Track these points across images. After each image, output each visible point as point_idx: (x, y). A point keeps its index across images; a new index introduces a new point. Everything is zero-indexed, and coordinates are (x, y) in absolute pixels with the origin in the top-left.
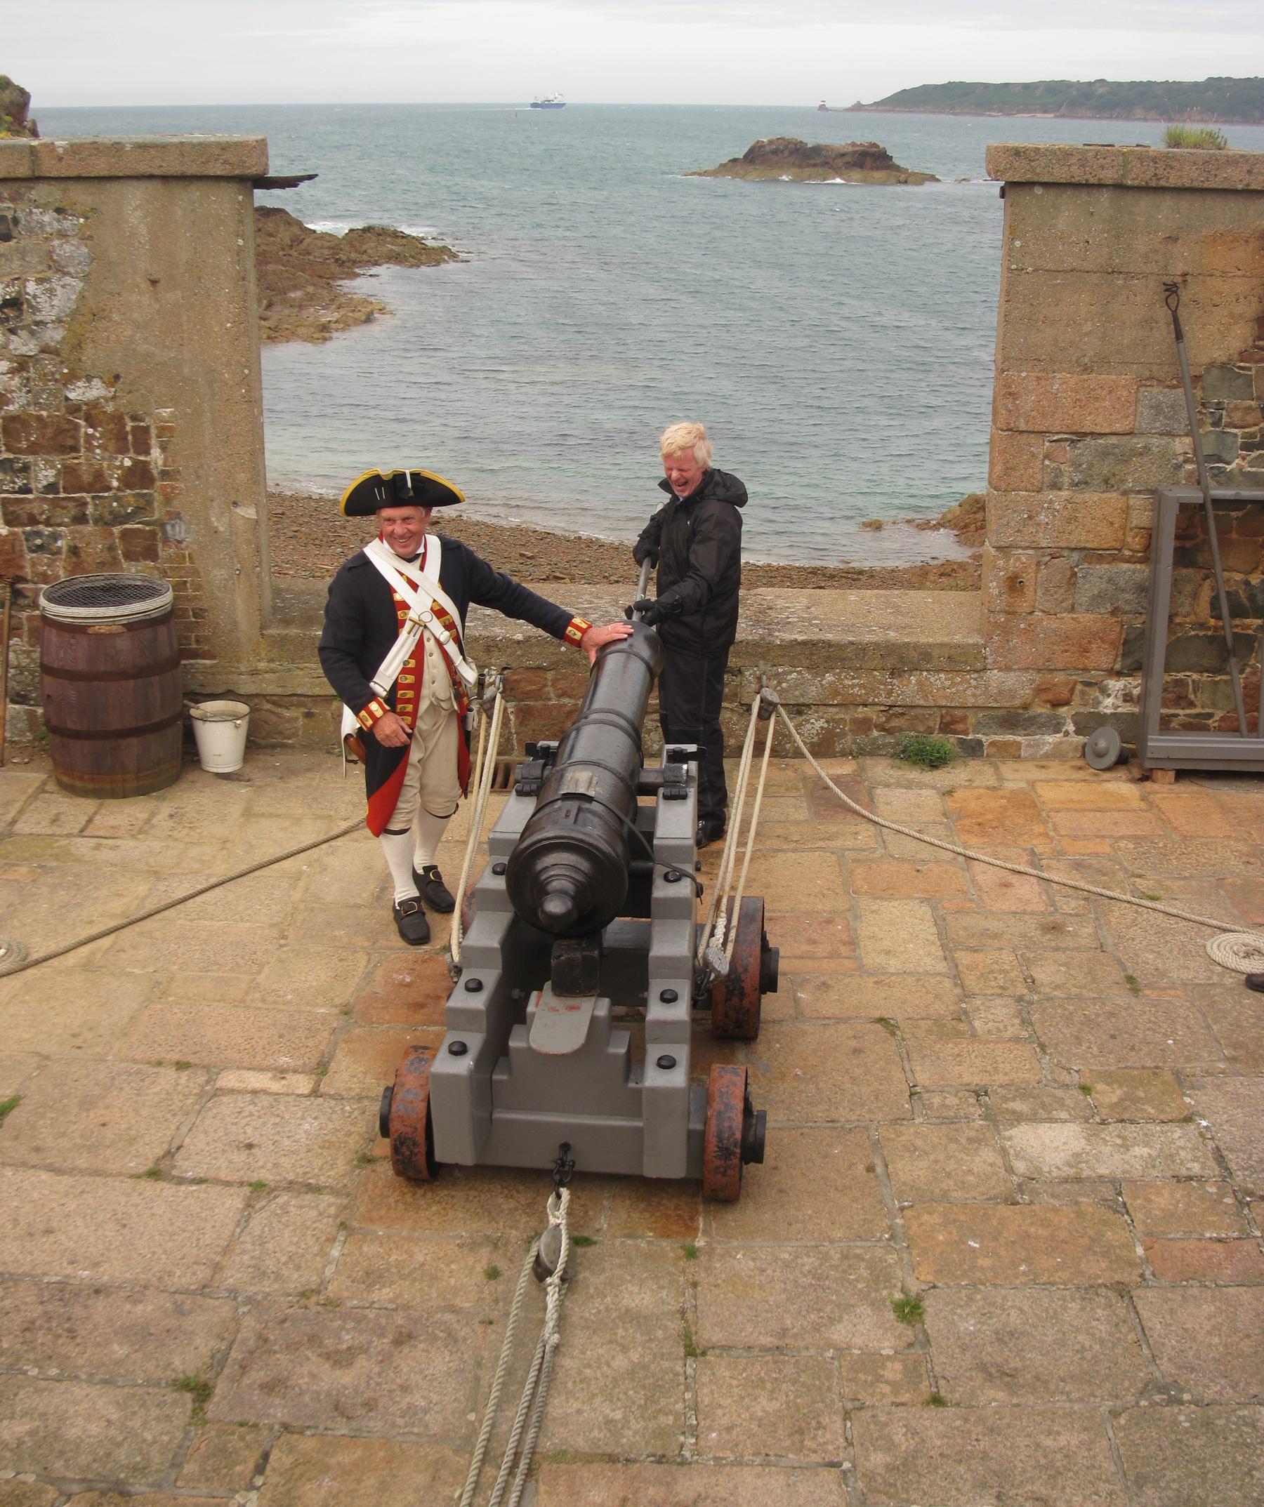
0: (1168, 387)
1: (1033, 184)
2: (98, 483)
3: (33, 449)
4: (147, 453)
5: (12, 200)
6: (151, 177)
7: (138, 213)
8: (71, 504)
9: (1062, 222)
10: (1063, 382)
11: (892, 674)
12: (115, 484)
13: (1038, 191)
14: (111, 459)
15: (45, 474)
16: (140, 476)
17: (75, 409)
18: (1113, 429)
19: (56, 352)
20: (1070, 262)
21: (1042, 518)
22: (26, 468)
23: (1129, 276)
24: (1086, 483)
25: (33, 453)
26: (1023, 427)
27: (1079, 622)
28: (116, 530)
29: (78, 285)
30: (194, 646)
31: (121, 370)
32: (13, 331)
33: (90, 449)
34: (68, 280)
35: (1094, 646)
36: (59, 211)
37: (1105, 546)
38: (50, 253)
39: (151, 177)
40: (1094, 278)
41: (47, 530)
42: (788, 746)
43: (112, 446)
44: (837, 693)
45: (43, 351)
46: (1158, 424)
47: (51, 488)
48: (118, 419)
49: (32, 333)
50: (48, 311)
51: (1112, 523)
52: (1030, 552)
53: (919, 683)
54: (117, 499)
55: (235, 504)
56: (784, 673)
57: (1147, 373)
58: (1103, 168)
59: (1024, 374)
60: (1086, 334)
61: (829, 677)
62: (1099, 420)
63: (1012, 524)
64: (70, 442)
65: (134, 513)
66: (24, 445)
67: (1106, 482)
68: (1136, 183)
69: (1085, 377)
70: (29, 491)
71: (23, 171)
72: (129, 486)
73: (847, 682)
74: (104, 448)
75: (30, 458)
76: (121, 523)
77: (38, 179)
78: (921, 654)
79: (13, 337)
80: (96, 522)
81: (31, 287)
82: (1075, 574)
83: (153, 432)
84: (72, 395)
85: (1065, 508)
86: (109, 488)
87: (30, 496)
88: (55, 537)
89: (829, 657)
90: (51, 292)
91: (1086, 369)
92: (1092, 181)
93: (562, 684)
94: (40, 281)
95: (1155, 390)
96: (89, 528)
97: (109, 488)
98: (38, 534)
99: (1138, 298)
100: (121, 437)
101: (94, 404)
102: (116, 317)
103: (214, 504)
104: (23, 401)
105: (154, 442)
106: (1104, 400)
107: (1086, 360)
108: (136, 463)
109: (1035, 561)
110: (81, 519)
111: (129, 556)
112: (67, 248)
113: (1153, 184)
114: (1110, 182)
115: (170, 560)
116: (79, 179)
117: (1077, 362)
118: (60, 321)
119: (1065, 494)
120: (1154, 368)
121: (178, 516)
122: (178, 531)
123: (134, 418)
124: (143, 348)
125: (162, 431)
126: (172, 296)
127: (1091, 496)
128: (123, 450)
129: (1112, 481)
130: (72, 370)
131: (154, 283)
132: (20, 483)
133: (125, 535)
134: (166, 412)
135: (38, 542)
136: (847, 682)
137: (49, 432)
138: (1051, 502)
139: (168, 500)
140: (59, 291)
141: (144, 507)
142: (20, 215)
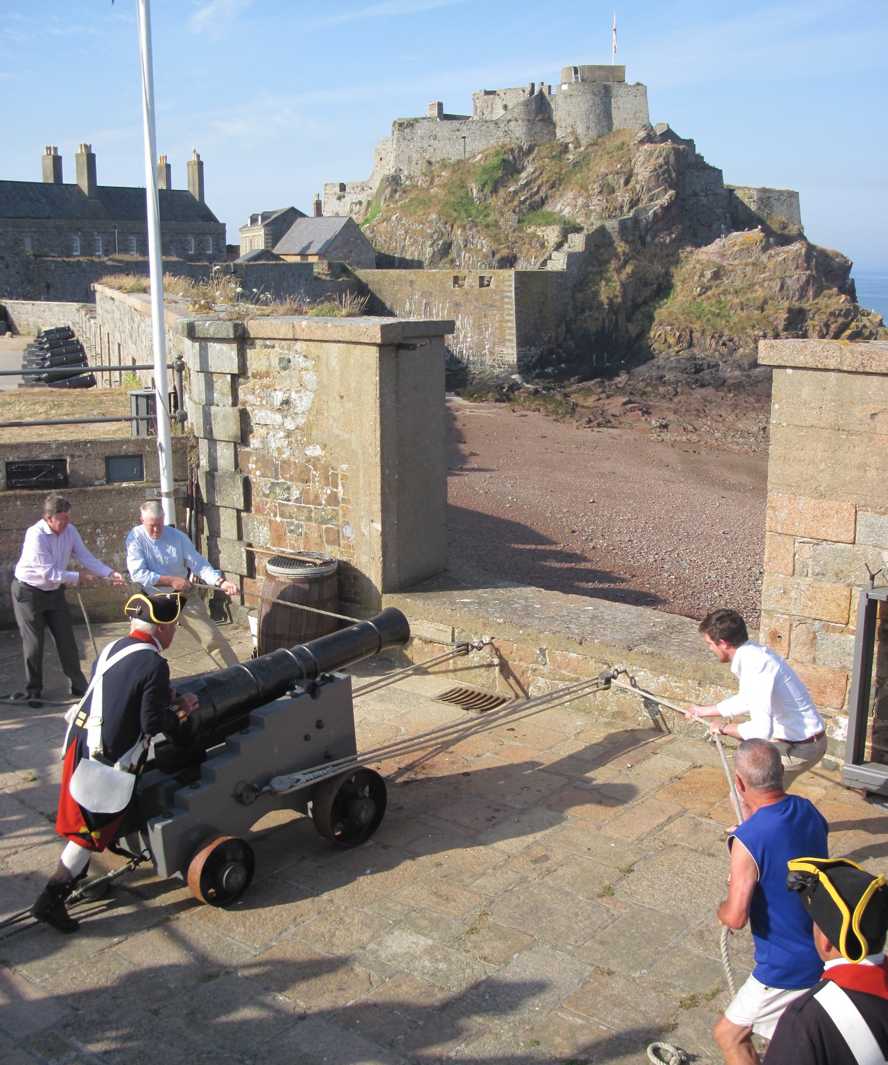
0: (878, 513)
1: (785, 367)
2: (316, 501)
3: (291, 479)
4: (337, 488)
5: (289, 349)
6: (339, 342)
7: (336, 360)
8: (306, 510)
9: (805, 393)
10: (805, 503)
11: (699, 683)
12: (324, 502)
13: (789, 371)
14: (322, 488)
15: (295, 493)
16: (333, 499)
17: (309, 461)
18: (839, 539)
19: (302, 429)
20: (810, 421)
21: (793, 594)
22: (288, 489)
23: (849, 433)
24: (823, 574)
25: (291, 480)
26: (780, 531)
27: (817, 672)
28: (324, 527)
29: (312, 396)
30: (353, 596)
31: (327, 442)
32: (286, 417)
33: (314, 482)
34: (308, 393)
35: (828, 690)
36: (305, 356)
37: (835, 620)
38: (301, 378)
39: (339, 342)
40: (826, 433)
41: (296, 522)
42: (640, 718)
43: (323, 482)
44: (666, 690)
45: (297, 428)
46: (871, 539)
47: (297, 500)
48: (326, 469)
49: (293, 418)
50: (299, 409)
51: (839, 605)
52: (787, 617)
53: (715, 693)
54: (323, 510)
55: (372, 521)
56: (636, 670)
57: (863, 502)
58: (827, 357)
59: (780, 495)
60: (821, 471)
61: (662, 679)
62: (830, 531)
63: (774, 595)
64: (306, 478)
65: (331, 519)
66: (288, 476)
67: (837, 575)
68: (850, 369)
69: (821, 501)
70: (289, 501)
71: (291, 337)
72: (330, 504)
73: (673, 684)
74: (319, 482)
75: (289, 483)
76: (325, 524)
77: (296, 340)
78: (716, 674)
79: (285, 420)
80: (316, 521)
81: (293, 395)
82: (815, 638)
83: (340, 476)
84: (308, 453)
85: (808, 590)
86: (320, 504)
87: (290, 503)
88: (299, 526)
89: (662, 665)
90: (301, 397)
91: (822, 496)
92: (820, 366)
93: (522, 653)
94: (297, 392)
95: (869, 514)
96: (313, 524)
97: (320, 504)
98: (292, 523)
99: (856, 449)
100: (327, 478)
101: (317, 459)
102: (326, 414)
103: (364, 520)
104: (288, 453)
105: (340, 482)
106: (833, 517)
107: (822, 489)
108: (332, 492)
109: (788, 624)
110: (309, 519)
111: (328, 542)
112: (308, 376)
113: (861, 370)
114: (832, 367)
115: (344, 547)
116: (310, 340)
117: (816, 489)
118: (303, 413)
119: (809, 580)
120: (868, 498)
121: (348, 523)
122: (348, 531)
123: (333, 468)
124: (337, 431)
125: (344, 477)
126: (349, 405)
127: (826, 585)
128: (327, 485)
129: (840, 576)
130: (308, 440)
131: (342, 397)
132: (286, 496)
133: (327, 529)
134: (345, 466)
135: (292, 528)
136: (673, 684)
137: (298, 471)
138: (798, 584)
139: (344, 515)
140: (304, 398)
141: (334, 517)
142: (291, 357)
